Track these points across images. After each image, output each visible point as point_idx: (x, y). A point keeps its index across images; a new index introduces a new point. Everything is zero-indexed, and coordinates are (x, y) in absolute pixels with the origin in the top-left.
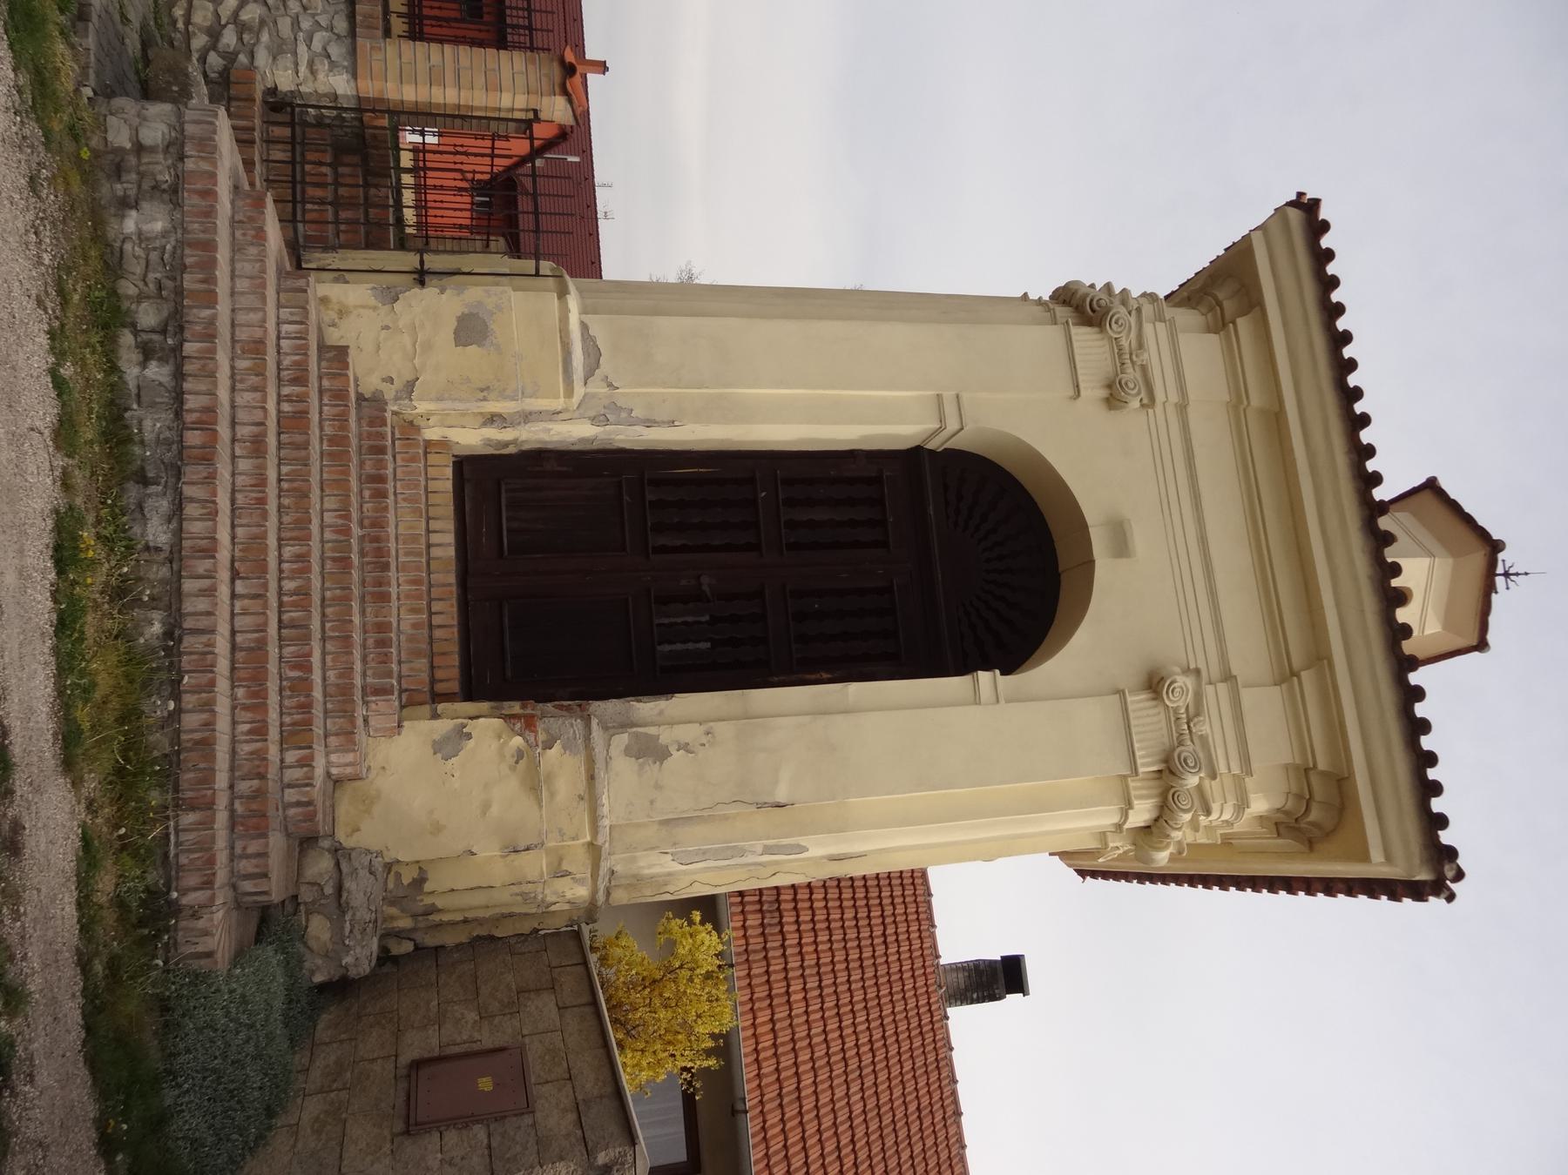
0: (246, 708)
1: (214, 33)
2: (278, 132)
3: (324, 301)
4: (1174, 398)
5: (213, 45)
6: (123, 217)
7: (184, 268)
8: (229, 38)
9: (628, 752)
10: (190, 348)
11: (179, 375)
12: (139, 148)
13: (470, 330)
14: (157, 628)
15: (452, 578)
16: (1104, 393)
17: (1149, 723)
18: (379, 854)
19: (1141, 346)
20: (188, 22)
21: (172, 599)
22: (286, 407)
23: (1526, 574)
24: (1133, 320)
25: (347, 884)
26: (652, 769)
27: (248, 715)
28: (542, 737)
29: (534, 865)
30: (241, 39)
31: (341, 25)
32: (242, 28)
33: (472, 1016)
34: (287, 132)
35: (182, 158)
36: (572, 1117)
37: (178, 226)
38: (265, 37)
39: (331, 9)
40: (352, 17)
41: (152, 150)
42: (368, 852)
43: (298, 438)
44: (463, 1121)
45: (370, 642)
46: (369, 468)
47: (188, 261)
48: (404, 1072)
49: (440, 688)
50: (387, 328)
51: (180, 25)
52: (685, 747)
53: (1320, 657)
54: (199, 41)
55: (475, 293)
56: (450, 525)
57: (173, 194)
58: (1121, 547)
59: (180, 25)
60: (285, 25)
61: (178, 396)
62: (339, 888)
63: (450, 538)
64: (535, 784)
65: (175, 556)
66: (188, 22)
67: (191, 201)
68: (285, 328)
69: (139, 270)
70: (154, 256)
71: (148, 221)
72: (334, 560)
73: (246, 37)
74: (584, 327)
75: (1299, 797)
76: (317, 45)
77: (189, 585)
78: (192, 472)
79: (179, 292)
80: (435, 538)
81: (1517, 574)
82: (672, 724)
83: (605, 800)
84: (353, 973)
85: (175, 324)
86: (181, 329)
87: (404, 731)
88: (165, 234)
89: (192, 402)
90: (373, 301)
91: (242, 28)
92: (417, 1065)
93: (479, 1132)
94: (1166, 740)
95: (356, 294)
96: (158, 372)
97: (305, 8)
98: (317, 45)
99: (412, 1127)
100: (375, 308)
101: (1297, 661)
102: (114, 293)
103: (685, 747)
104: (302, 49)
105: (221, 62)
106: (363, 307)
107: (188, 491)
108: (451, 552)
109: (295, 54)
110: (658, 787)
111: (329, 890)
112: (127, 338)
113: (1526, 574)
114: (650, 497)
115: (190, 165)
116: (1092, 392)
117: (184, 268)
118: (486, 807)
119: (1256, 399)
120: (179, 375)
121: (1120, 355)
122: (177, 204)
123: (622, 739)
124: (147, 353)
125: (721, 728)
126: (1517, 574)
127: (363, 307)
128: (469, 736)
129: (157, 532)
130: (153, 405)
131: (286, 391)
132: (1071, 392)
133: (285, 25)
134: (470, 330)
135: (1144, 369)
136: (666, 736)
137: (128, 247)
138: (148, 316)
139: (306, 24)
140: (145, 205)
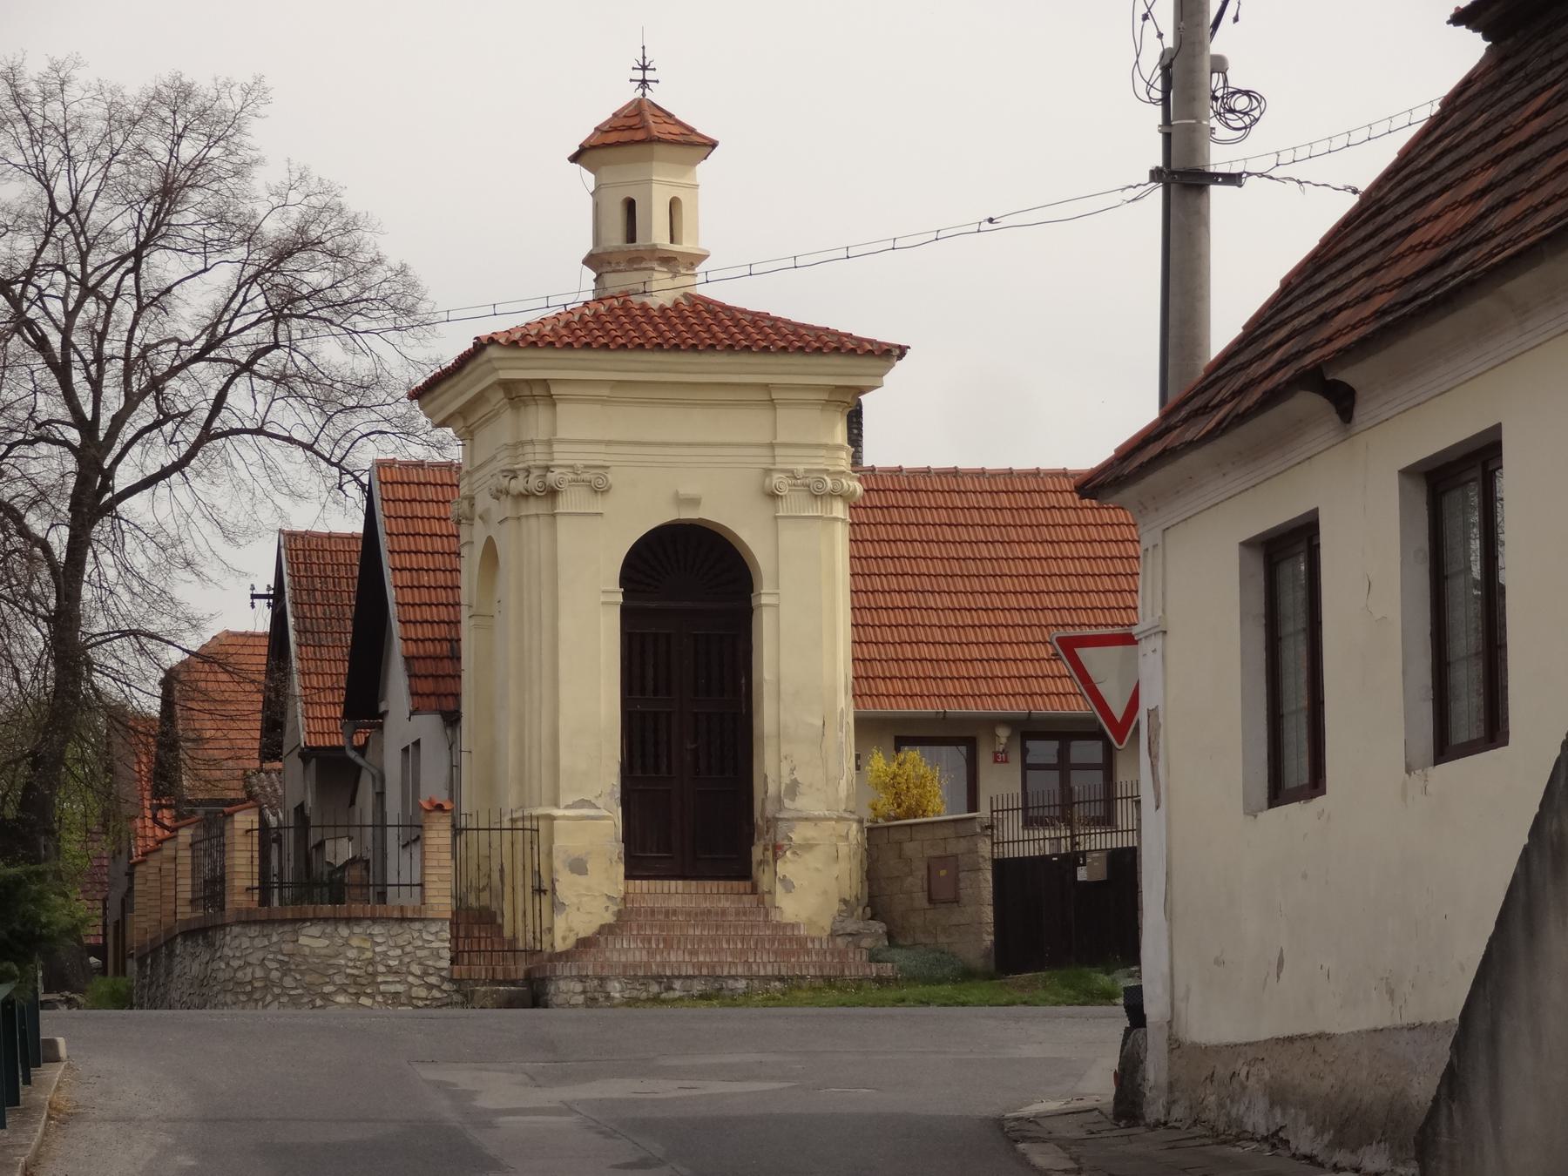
0: (799, 957)
1: (430, 987)
2: (466, 961)
3: (564, 939)
4: (602, 448)
5: (438, 987)
6: (613, 998)
7: (636, 975)
8: (433, 980)
9: (793, 800)
10: (668, 973)
11: (679, 977)
12: (584, 992)
13: (579, 867)
14: (777, 983)
15: (694, 883)
16: (599, 497)
17: (794, 504)
18: (834, 918)
19: (571, 467)
21: (767, 979)
22: (661, 946)
23: (643, 47)
24: (557, 471)
25: (848, 931)
26: (802, 789)
27: (802, 957)
28: (786, 842)
29: (844, 848)
30: (431, 975)
31: (417, 925)
32: (426, 973)
33: (910, 879)
34: (466, 955)
35: (587, 976)
36: (961, 840)
37: (617, 978)
38: (430, 963)
39: (408, 931)
40: (412, 920)
41: (585, 987)
42: (833, 923)
43: (675, 942)
45: (744, 918)
46: (661, 917)
47: (632, 973)
48: (932, 906)
49: (749, 890)
50: (578, 909)
51: (428, 1002)
52: (792, 770)
53: (766, 387)
55: (557, 864)
56: (666, 882)
57: (602, 980)
58: (694, 502)
59: (428, 1002)
60: (420, 953)
61: (688, 977)
62: (850, 934)
63: (673, 883)
64: (808, 846)
65: (750, 978)
66: (427, 999)
67: (606, 973)
68: (625, 946)
69: (636, 992)
70: (629, 986)
71: (615, 989)
72: (717, 930)
73: (431, 972)
74: (567, 807)
75: (839, 406)
76: (431, 938)
77: (762, 973)
78: (718, 972)
79: (645, 977)
80: (666, 891)
81: (644, 57)
82: (780, 776)
83: (816, 813)
84: (885, 930)
85: (658, 978)
86: (661, 977)
87: (781, 905)
88: (620, 982)
89: (690, 972)
90: (564, 915)
91: (426, 973)
94: (805, 493)
95: (560, 924)
96: (677, 984)
97: (410, 943)
98: (431, 938)
100: (567, 914)
101: (764, 396)
102: (648, 999)
103: (792, 770)
104: (434, 945)
105: (446, 984)
106: (567, 919)
107: (725, 973)
108: (680, 882)
109: (438, 948)
110: (810, 786)
111: (850, 939)
112: (664, 995)
113: (643, 47)
114: (639, 775)
115: (590, 973)
116: (598, 505)
117: (636, 975)
118: (817, 870)
119: (605, 392)
120: (679, 977)
121: (577, 481)
122: (607, 978)
123: (787, 803)
124: (670, 988)
125: (784, 751)
126: (644, 57)
127: (567, 919)
128: (784, 876)
129: (742, 984)
130: (691, 986)
131: (654, 946)
132: (599, 518)
133: (420, 953)
134: (579, 867)
135: (586, 467)
136: (786, 780)
137: (626, 996)
138: (654, 988)
139: (420, 943)
140: (608, 990)
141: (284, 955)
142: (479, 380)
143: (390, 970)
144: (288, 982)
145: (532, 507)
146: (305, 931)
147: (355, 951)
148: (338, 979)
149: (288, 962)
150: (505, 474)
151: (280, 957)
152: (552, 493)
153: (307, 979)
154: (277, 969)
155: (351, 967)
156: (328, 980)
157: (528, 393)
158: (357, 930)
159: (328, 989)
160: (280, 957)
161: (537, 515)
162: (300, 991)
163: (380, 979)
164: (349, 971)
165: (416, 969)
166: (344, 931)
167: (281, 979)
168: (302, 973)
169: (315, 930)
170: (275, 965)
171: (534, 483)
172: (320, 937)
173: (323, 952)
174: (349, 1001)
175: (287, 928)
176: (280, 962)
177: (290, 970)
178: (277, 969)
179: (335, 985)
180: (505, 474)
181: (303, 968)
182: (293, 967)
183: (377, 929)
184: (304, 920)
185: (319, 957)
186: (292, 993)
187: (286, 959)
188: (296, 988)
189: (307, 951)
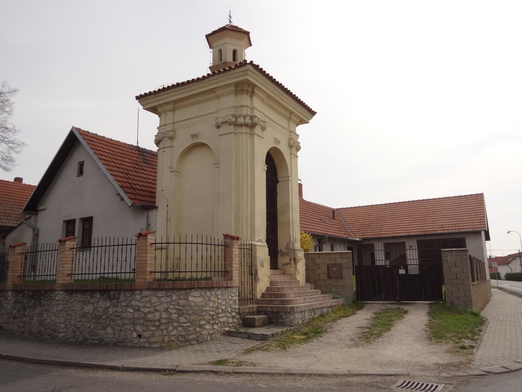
1: (233, 317)
13: (262, 266)
20: (232, 323)
33: (319, 270)
36: (343, 259)
44: (341, 272)
48: (329, 279)
51: (233, 325)
54: (235, 320)
59: (233, 325)
66: (232, 323)
92: (329, 277)
93: (343, 270)
99: (341, 278)
135: (261, 121)
139: (230, 298)
141: (180, 306)
142: (217, 83)
143: (223, 311)
144: (182, 319)
145: (244, 130)
146: (191, 294)
147: (212, 303)
148: (207, 317)
149: (182, 310)
150: (233, 116)
151: (177, 307)
152: (252, 126)
153: (192, 317)
154: (175, 313)
155: (211, 311)
156: (202, 318)
157: (246, 89)
158: (213, 293)
159: (202, 322)
160: (177, 307)
161: (246, 133)
162: (188, 324)
163: (220, 316)
164: (211, 313)
165: (229, 310)
166: (208, 294)
167: (178, 318)
168: (189, 315)
169: (197, 293)
170: (175, 311)
171: (248, 120)
172: (198, 297)
173: (200, 304)
174: (210, 328)
175: (182, 292)
176: (176, 309)
177: (183, 313)
178: (175, 313)
179: (205, 320)
180: (233, 116)
181: (190, 312)
182: (185, 312)
183: (219, 292)
184: (191, 289)
185: (198, 306)
186: (184, 325)
187: (181, 308)
188: (186, 323)
189: (193, 304)
